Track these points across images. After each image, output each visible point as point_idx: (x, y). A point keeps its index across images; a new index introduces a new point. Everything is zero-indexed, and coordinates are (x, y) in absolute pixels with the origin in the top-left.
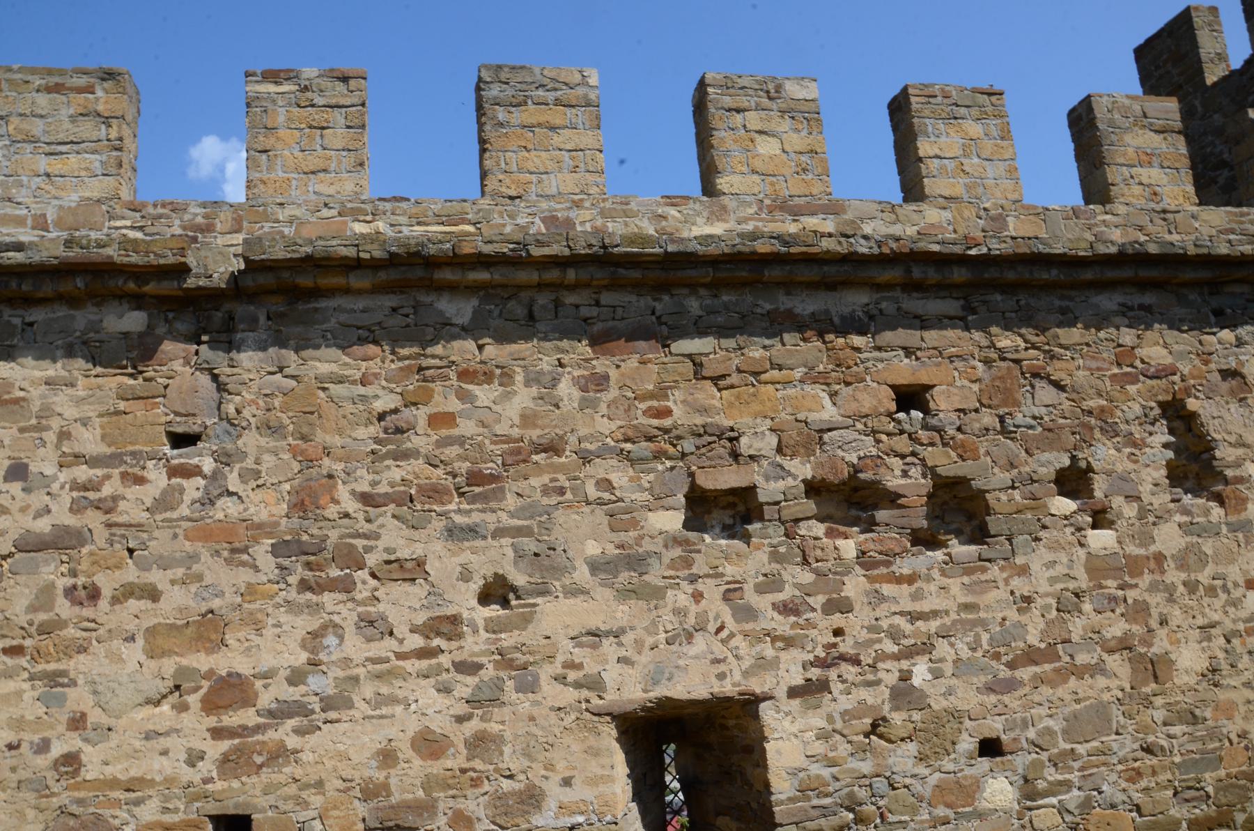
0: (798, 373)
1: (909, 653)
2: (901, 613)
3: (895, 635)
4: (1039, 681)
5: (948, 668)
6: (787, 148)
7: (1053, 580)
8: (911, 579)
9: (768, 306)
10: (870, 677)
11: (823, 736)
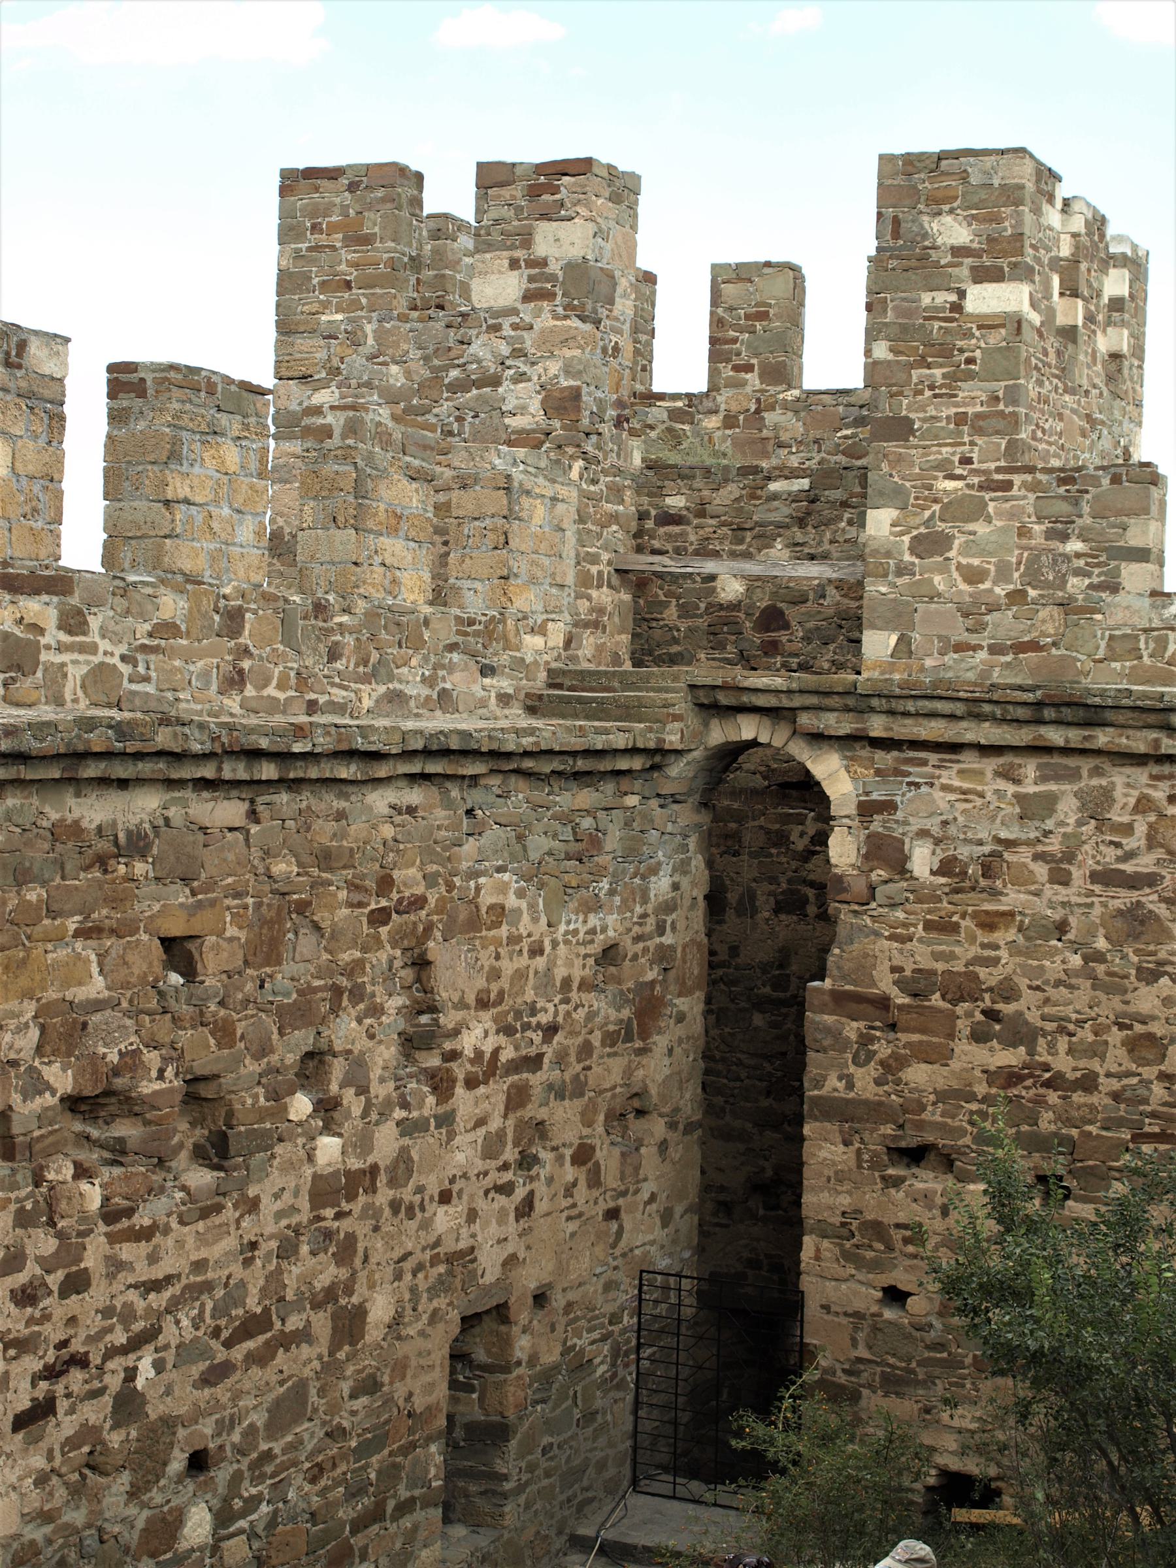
0: (72, 923)
1: (135, 1344)
2: (135, 1286)
3: (127, 1315)
4: (253, 1359)
5: (170, 1356)
6: (19, 466)
7: (279, 1215)
8: (145, 1234)
9: (55, 816)
10: (97, 1384)
11: (42, 1480)
